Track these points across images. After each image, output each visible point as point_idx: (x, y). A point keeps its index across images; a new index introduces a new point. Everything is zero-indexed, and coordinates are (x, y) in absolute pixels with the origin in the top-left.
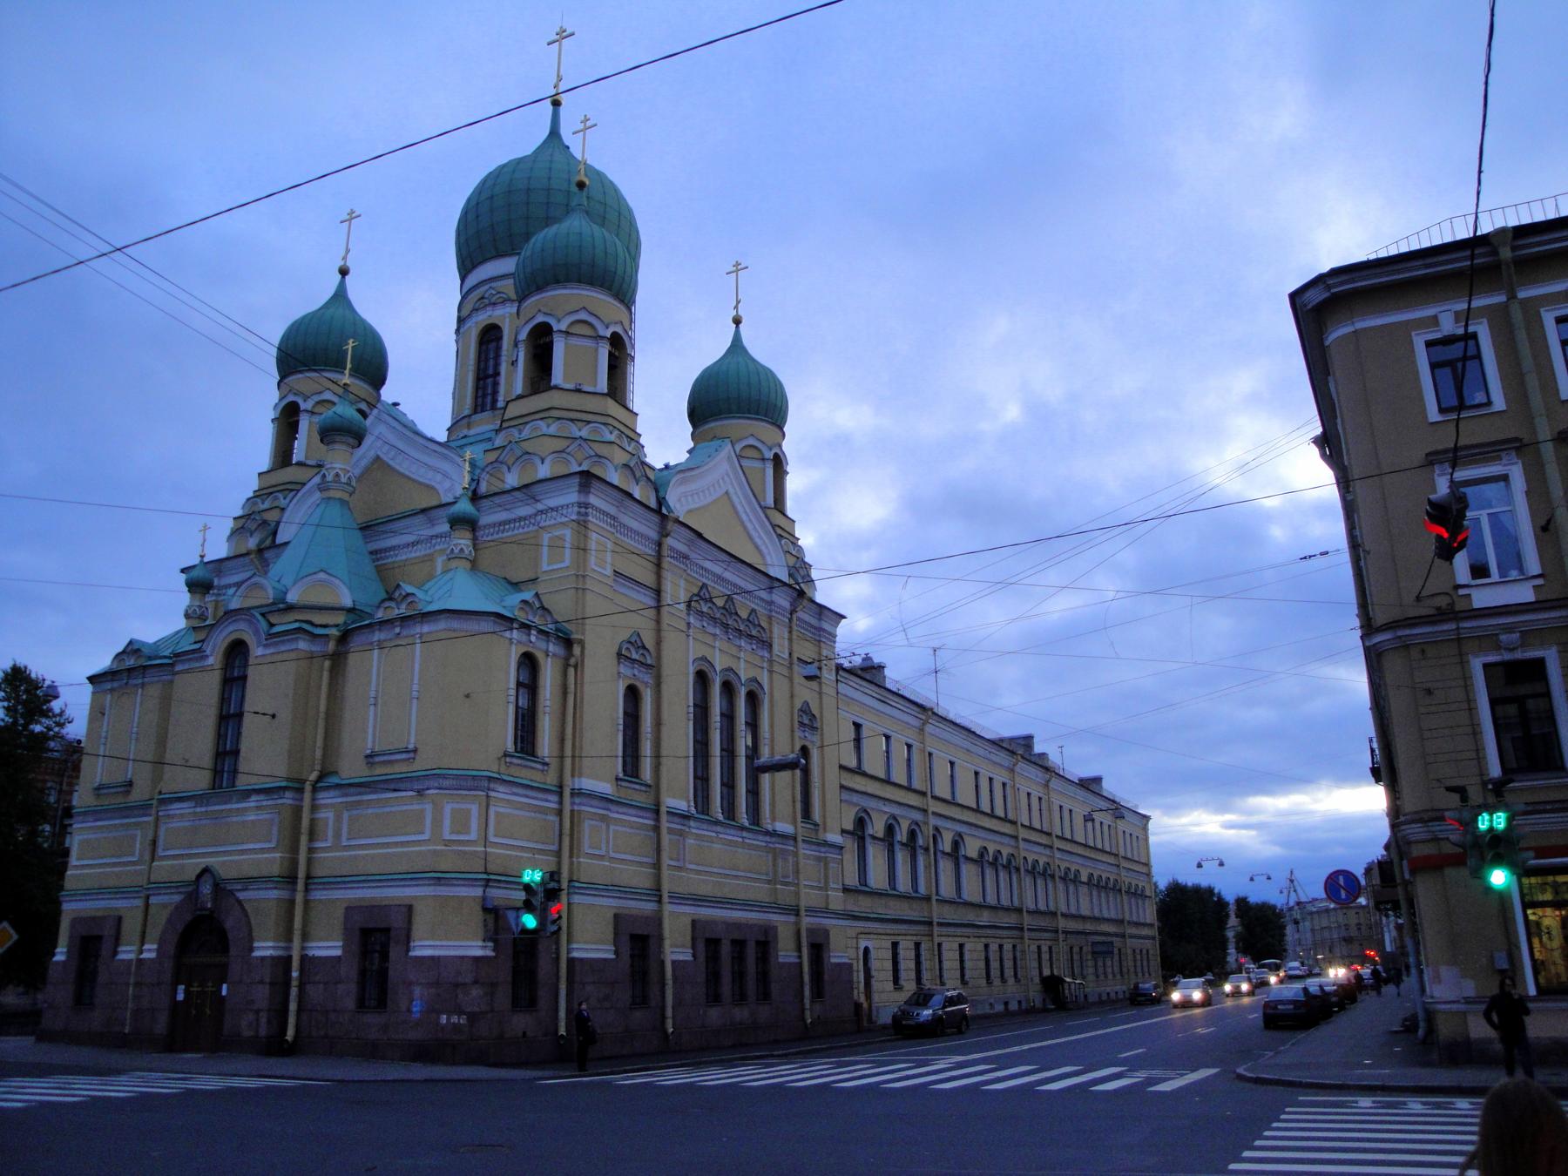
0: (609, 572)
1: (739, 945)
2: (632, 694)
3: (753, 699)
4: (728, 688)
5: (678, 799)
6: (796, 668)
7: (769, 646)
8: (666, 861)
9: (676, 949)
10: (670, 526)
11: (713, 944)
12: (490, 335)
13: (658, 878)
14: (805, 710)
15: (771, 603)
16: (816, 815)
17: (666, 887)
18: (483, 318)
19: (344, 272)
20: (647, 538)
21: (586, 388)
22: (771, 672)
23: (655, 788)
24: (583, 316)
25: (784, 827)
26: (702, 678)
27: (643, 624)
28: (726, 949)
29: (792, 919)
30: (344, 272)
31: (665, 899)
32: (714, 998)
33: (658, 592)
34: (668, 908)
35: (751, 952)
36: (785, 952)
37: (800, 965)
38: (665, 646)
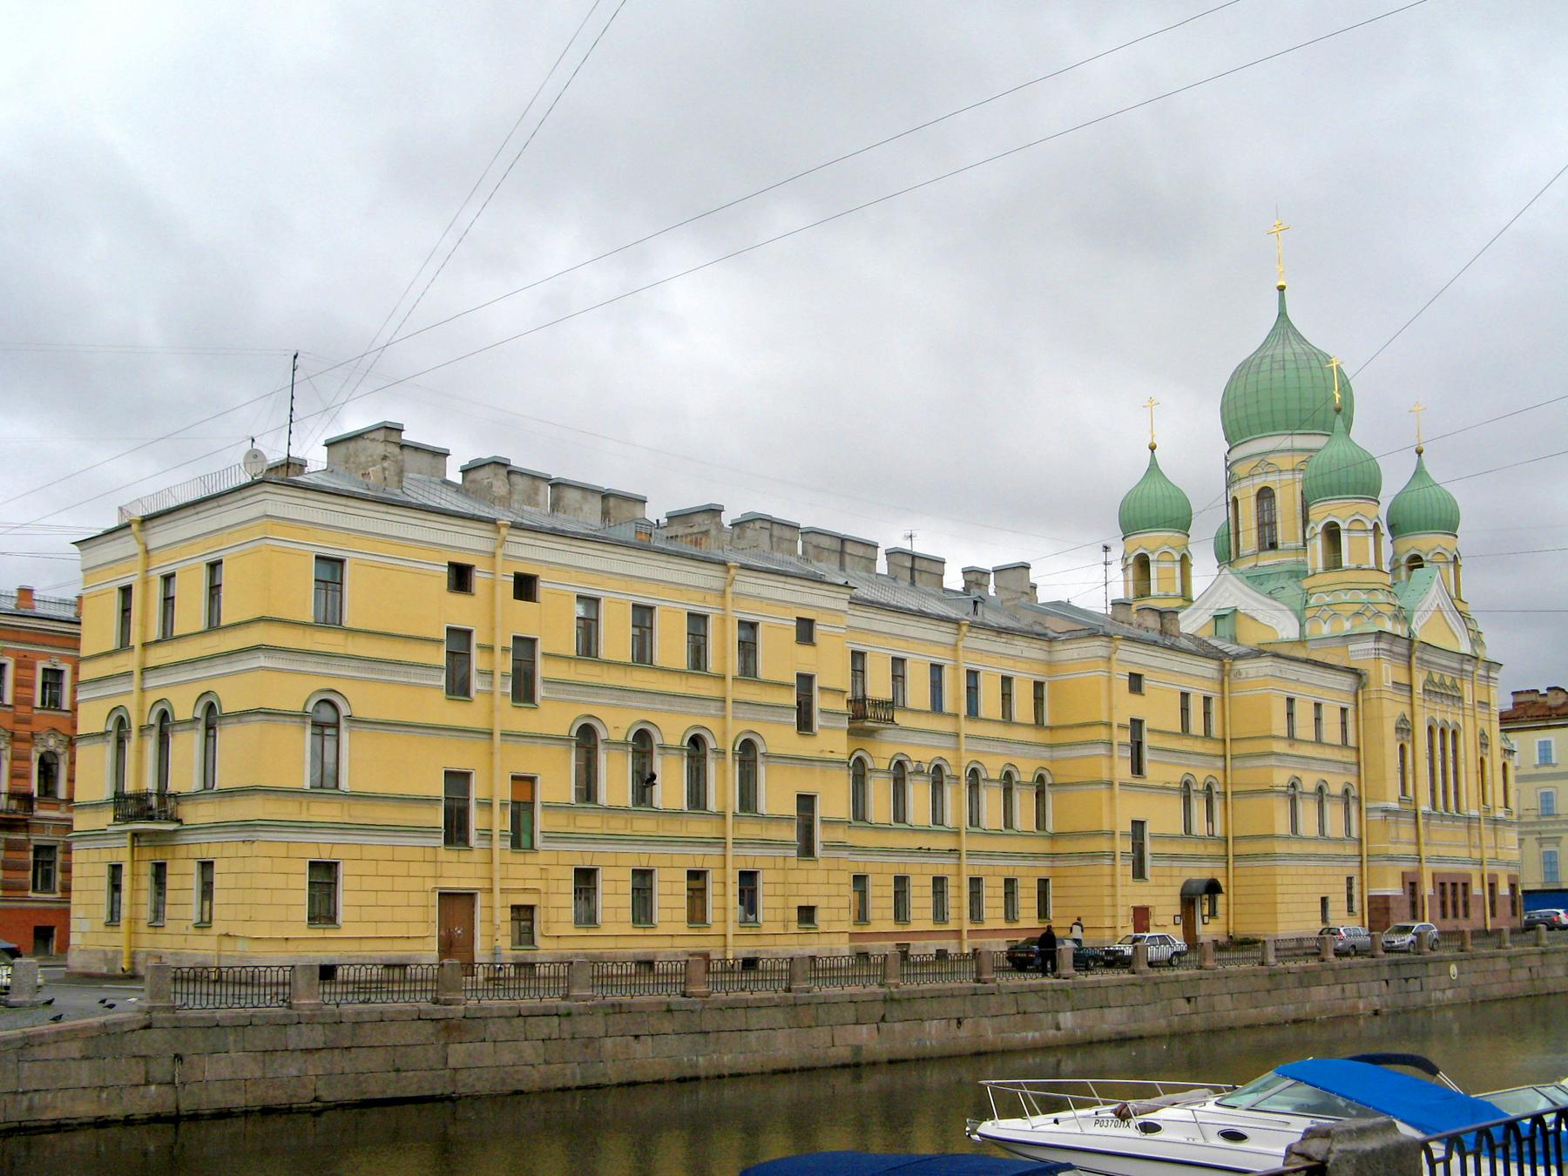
0: (1390, 684)
1: (1454, 885)
2: (1402, 747)
3: (1454, 733)
4: (1442, 731)
5: (1425, 807)
6: (1478, 710)
7: (1461, 699)
8: (1422, 840)
9: (1427, 889)
10: (1416, 645)
11: (1443, 884)
12: (1265, 495)
13: (1419, 850)
14: (1483, 734)
15: (1462, 670)
16: (1489, 802)
17: (1423, 856)
18: (1260, 482)
19: (1152, 448)
20: (1402, 655)
21: (1363, 567)
22: (1463, 715)
23: (1414, 801)
24: (1357, 517)
25: (1474, 812)
26: (1430, 729)
27: (1406, 709)
28: (1449, 888)
29: (1478, 867)
30: (1152, 448)
31: (1424, 861)
32: (1444, 916)
33: (1411, 686)
34: (1425, 865)
35: (1460, 888)
36: (1476, 889)
37: (1484, 896)
38: (1417, 719)
